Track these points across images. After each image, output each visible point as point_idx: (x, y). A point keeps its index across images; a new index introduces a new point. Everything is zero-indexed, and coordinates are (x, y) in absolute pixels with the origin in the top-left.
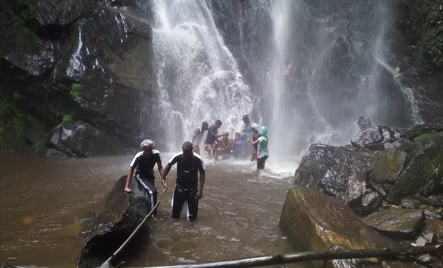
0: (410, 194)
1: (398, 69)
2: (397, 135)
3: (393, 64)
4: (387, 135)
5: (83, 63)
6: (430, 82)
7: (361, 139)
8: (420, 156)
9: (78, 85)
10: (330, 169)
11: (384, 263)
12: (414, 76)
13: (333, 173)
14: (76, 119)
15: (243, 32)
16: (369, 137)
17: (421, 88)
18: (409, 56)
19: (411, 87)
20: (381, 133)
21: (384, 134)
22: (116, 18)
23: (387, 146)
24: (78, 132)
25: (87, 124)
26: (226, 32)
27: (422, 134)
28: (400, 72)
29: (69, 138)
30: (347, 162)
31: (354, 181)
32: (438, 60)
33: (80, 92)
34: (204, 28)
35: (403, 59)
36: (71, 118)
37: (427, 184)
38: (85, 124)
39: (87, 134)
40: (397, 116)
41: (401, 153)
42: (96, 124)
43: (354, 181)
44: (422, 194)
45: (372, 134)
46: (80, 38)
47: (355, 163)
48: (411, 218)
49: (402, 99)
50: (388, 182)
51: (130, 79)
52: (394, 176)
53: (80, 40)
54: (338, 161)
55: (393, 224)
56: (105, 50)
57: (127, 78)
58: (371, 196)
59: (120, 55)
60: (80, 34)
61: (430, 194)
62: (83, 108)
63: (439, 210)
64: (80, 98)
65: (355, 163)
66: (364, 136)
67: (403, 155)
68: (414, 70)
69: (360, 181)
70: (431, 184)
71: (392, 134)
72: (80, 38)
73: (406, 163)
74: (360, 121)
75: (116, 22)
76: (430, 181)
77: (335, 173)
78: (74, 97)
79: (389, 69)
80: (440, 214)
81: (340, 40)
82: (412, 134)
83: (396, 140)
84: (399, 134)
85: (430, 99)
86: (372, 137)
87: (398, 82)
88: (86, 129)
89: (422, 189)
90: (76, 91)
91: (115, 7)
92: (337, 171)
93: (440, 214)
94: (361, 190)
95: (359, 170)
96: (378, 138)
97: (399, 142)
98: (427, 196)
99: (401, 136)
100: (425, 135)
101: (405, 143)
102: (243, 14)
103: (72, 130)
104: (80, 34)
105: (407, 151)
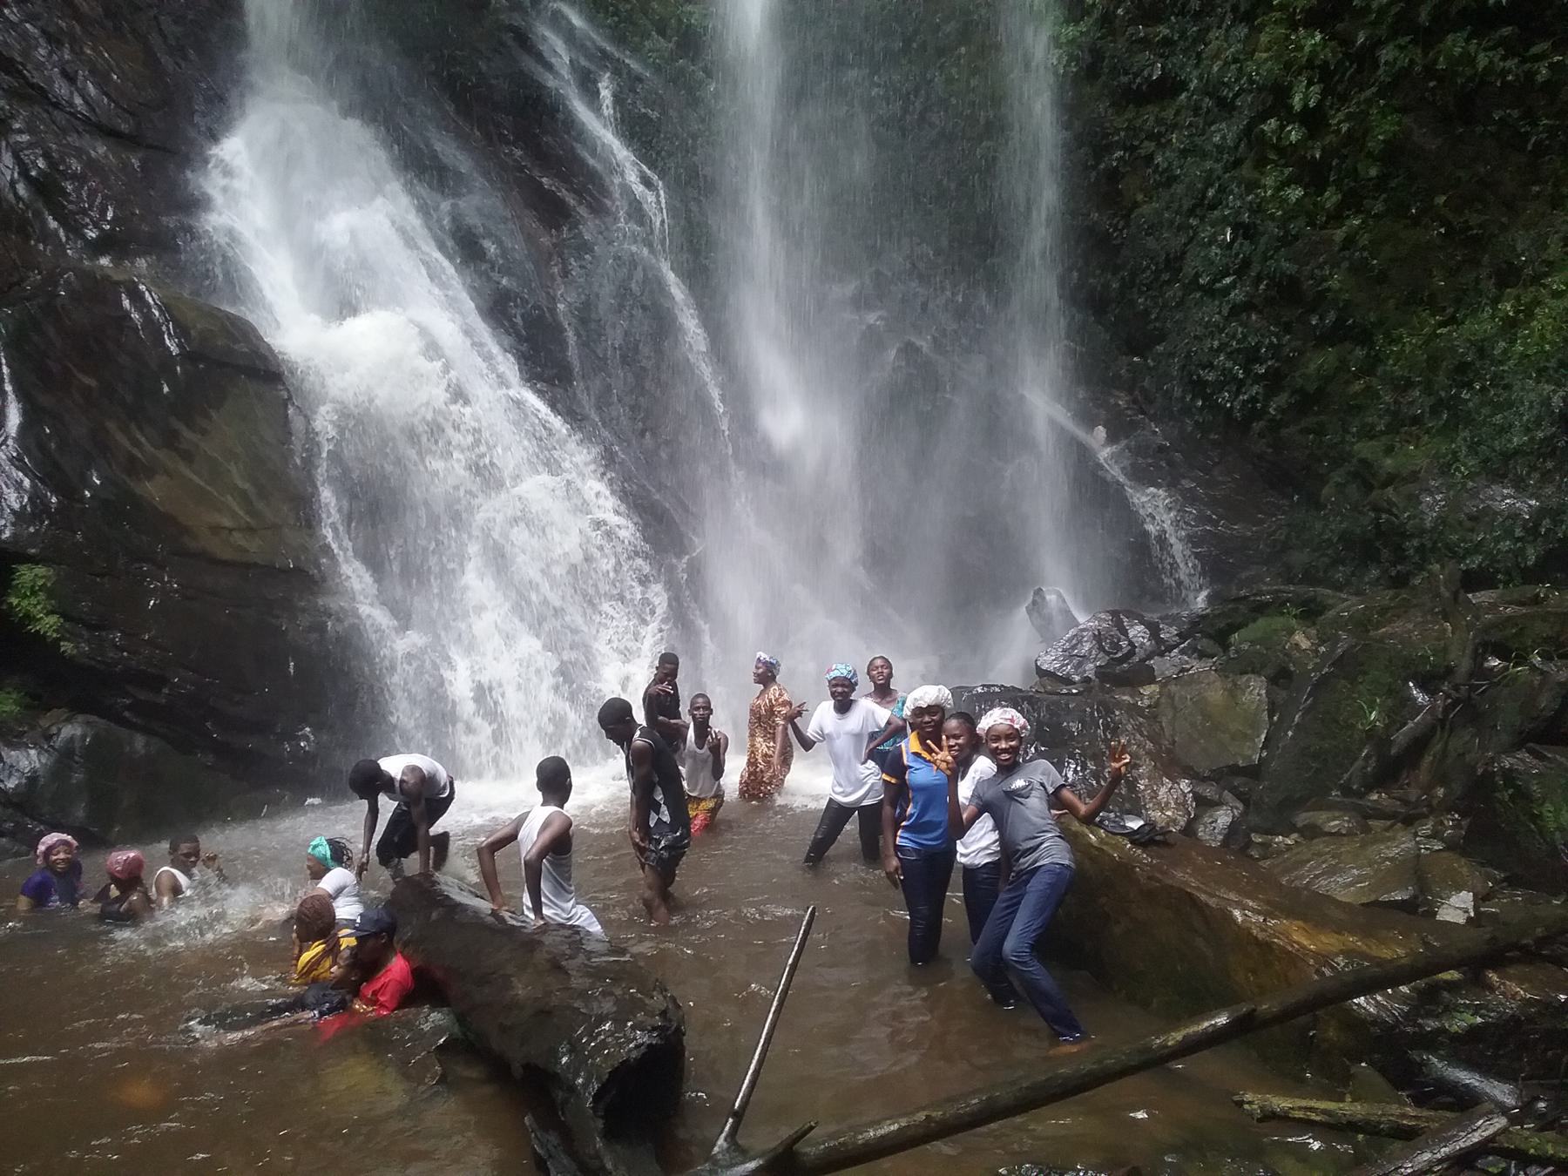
0: (1315, 797)
1: (1101, 431)
2: (1169, 633)
3: (1089, 422)
4: (1137, 632)
5: (40, 480)
6: (1215, 464)
7: (1069, 654)
8: (1323, 682)
9: (41, 570)
10: (1072, 756)
11: (1493, 977)
12: (1161, 449)
13: (1084, 768)
14: (38, 703)
15: (578, 335)
16: (1090, 650)
17: (1187, 484)
18: (1130, 391)
19: (1158, 486)
20: (1125, 633)
21: (1131, 633)
22: (126, 303)
24: (66, 755)
25: (95, 718)
26: (520, 338)
27: (1254, 620)
28: (1112, 439)
29: (33, 779)
30: (1106, 726)
31: (1155, 780)
32: (1237, 396)
33: (49, 598)
34: (447, 328)
35: (1112, 401)
36: (15, 702)
37: (1356, 759)
38: (80, 718)
39: (99, 757)
40: (1137, 574)
41: (1249, 680)
42: (127, 714)
43: (1155, 780)
44: (1346, 790)
45: (1098, 638)
46: (8, 388)
47: (1129, 727)
48: (1391, 859)
49: (1129, 519)
50: (1235, 770)
51: (231, 530)
52: (1253, 752)
53: (11, 397)
54: (1075, 727)
55: (1352, 884)
56: (111, 425)
57: (216, 529)
58: (1223, 818)
59: (170, 440)
60: (5, 370)
61: (1370, 789)
62: (72, 657)
63: (1427, 828)
64: (53, 619)
65: (1129, 727)
66: (1074, 647)
67: (1256, 690)
68: (1156, 433)
69: (1174, 780)
70: (1368, 757)
71: (1154, 630)
72: (8, 388)
74: (1034, 603)
75: (127, 315)
76: (1361, 751)
77: (1091, 766)
78: (29, 618)
79: (1081, 434)
80: (1435, 835)
81: (909, 350)
83: (1170, 649)
84: (1174, 630)
85: (1221, 517)
86: (1101, 649)
87: (1115, 472)
88: (95, 737)
89: (1346, 776)
90: (34, 593)
91: (104, 261)
92: (1094, 757)
93: (1435, 835)
94: (1181, 805)
95: (1149, 745)
97: (1182, 652)
98: (1362, 796)
99: (1182, 636)
100: (1262, 624)
101: (1237, 652)
102: (565, 273)
103: (36, 745)
104: (5, 370)
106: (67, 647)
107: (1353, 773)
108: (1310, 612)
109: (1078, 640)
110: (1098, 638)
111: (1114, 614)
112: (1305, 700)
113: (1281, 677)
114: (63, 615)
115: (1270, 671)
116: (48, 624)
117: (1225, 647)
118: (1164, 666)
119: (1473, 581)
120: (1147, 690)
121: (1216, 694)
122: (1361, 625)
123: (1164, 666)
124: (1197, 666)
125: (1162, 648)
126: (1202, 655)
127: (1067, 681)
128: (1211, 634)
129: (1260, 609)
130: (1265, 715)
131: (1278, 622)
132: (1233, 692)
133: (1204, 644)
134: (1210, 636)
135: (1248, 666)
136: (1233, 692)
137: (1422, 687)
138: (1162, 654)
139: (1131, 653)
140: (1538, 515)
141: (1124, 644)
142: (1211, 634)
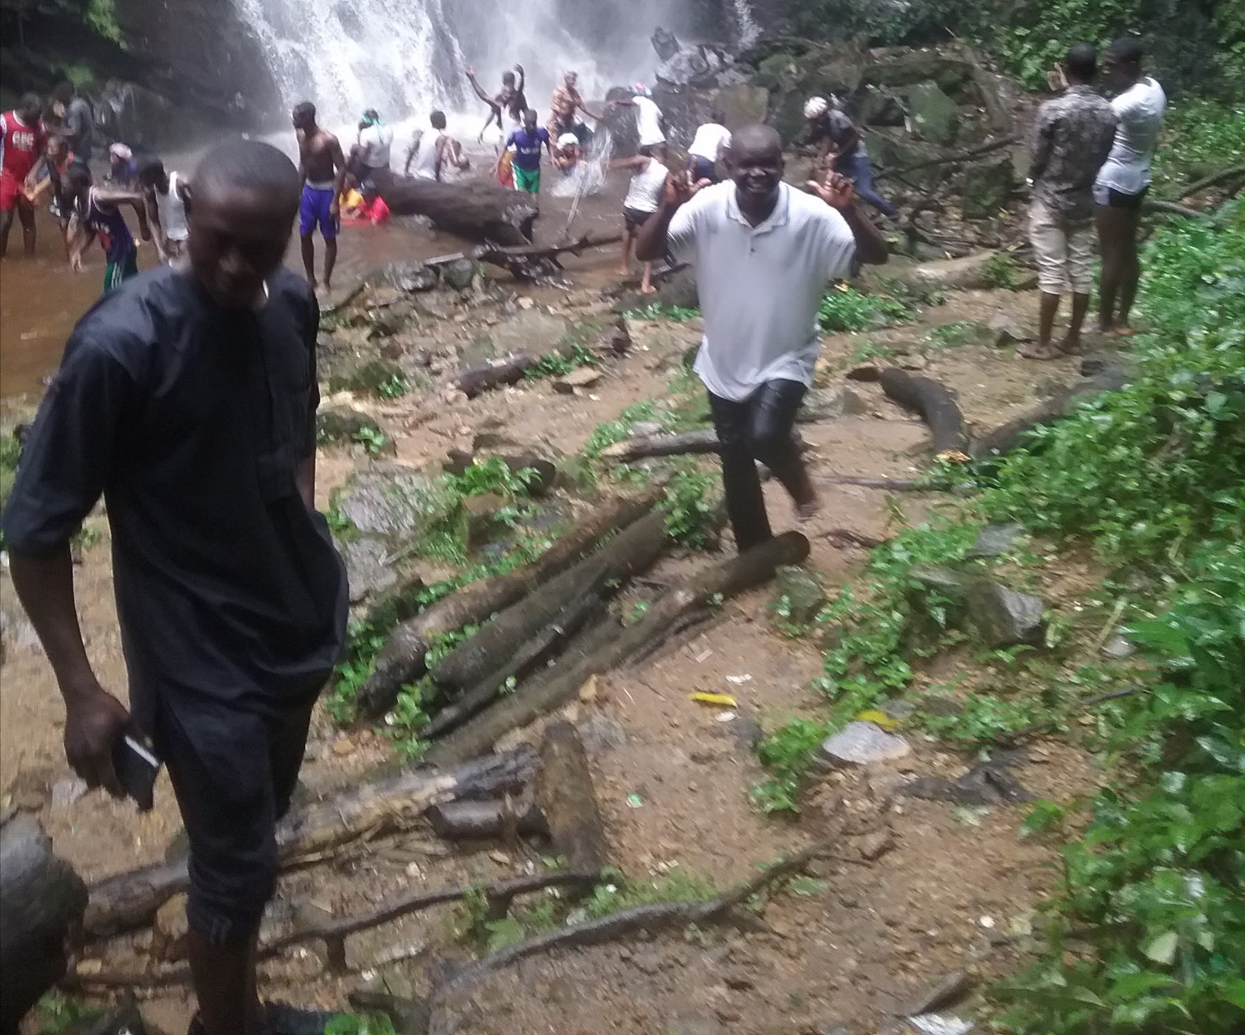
2: (729, 58)
4: (712, 58)
7: (674, 69)
8: (792, 93)
20: (704, 57)
23: (719, 77)
45: (691, 60)
67: (763, 94)
71: (721, 56)
73: (770, 104)
82: (755, 56)
84: (732, 57)
96: (700, 65)
99: (736, 61)
100: (775, 59)
105: (764, 85)
106: (123, 45)
107: (799, 138)
108: (800, 51)
109: (680, 60)
110: (691, 60)
111: (700, 47)
112: (782, 102)
113: (775, 90)
114: (121, 27)
115: (772, 85)
116: (113, 32)
117: (757, 69)
118: (724, 79)
119: (875, 43)
120: (714, 92)
121: (744, 96)
122: (817, 64)
123: (724, 79)
124: (742, 78)
125: (724, 67)
126: (745, 72)
127: (673, 84)
128: (751, 60)
129: (775, 50)
130: (765, 108)
131: (783, 57)
132: (753, 96)
133: (747, 67)
134: (748, 62)
135: (761, 82)
136: (753, 96)
137: (838, 97)
138: (722, 71)
139: (708, 69)
140: (909, 10)
141: (704, 65)
142: (751, 60)
